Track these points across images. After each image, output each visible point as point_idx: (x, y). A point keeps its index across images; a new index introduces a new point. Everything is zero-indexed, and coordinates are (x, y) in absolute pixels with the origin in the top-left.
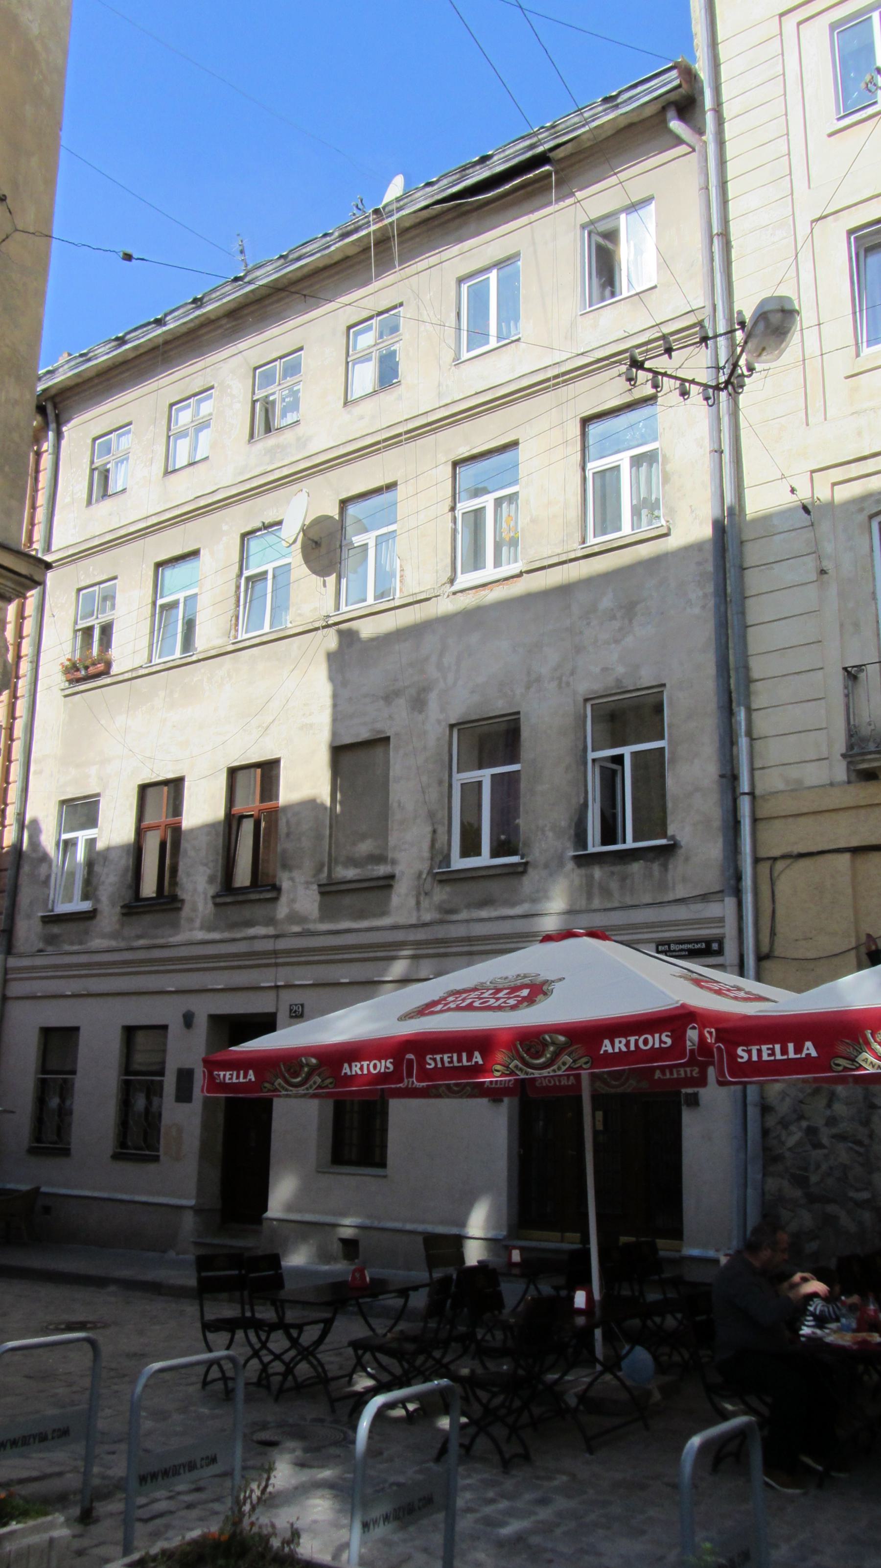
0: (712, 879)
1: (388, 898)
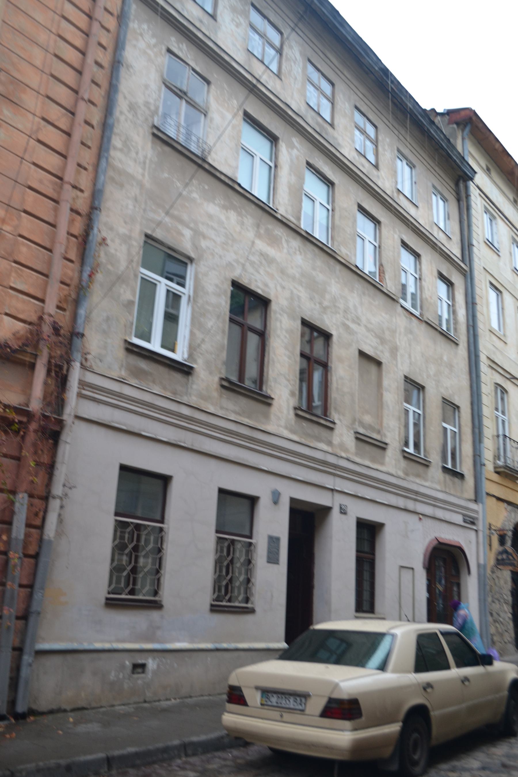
1: (384, 457)
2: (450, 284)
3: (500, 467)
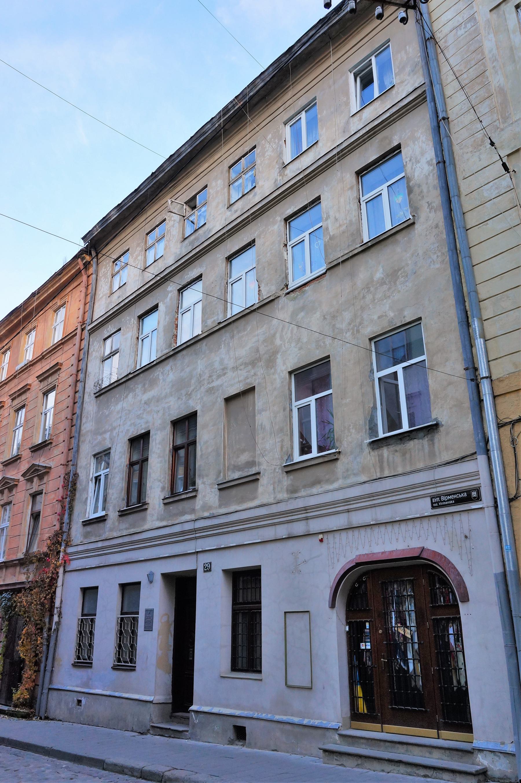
0: (468, 445)
1: (256, 489)
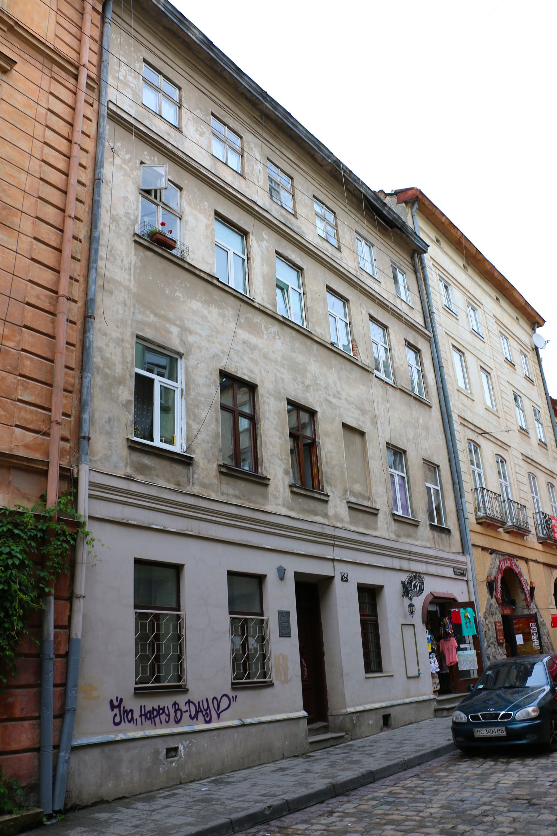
1: (376, 522)
2: (417, 351)
3: (482, 518)
